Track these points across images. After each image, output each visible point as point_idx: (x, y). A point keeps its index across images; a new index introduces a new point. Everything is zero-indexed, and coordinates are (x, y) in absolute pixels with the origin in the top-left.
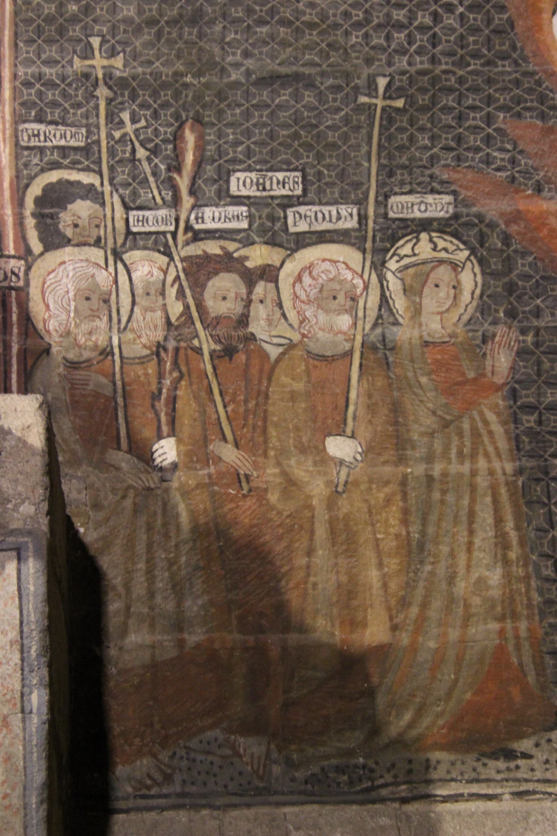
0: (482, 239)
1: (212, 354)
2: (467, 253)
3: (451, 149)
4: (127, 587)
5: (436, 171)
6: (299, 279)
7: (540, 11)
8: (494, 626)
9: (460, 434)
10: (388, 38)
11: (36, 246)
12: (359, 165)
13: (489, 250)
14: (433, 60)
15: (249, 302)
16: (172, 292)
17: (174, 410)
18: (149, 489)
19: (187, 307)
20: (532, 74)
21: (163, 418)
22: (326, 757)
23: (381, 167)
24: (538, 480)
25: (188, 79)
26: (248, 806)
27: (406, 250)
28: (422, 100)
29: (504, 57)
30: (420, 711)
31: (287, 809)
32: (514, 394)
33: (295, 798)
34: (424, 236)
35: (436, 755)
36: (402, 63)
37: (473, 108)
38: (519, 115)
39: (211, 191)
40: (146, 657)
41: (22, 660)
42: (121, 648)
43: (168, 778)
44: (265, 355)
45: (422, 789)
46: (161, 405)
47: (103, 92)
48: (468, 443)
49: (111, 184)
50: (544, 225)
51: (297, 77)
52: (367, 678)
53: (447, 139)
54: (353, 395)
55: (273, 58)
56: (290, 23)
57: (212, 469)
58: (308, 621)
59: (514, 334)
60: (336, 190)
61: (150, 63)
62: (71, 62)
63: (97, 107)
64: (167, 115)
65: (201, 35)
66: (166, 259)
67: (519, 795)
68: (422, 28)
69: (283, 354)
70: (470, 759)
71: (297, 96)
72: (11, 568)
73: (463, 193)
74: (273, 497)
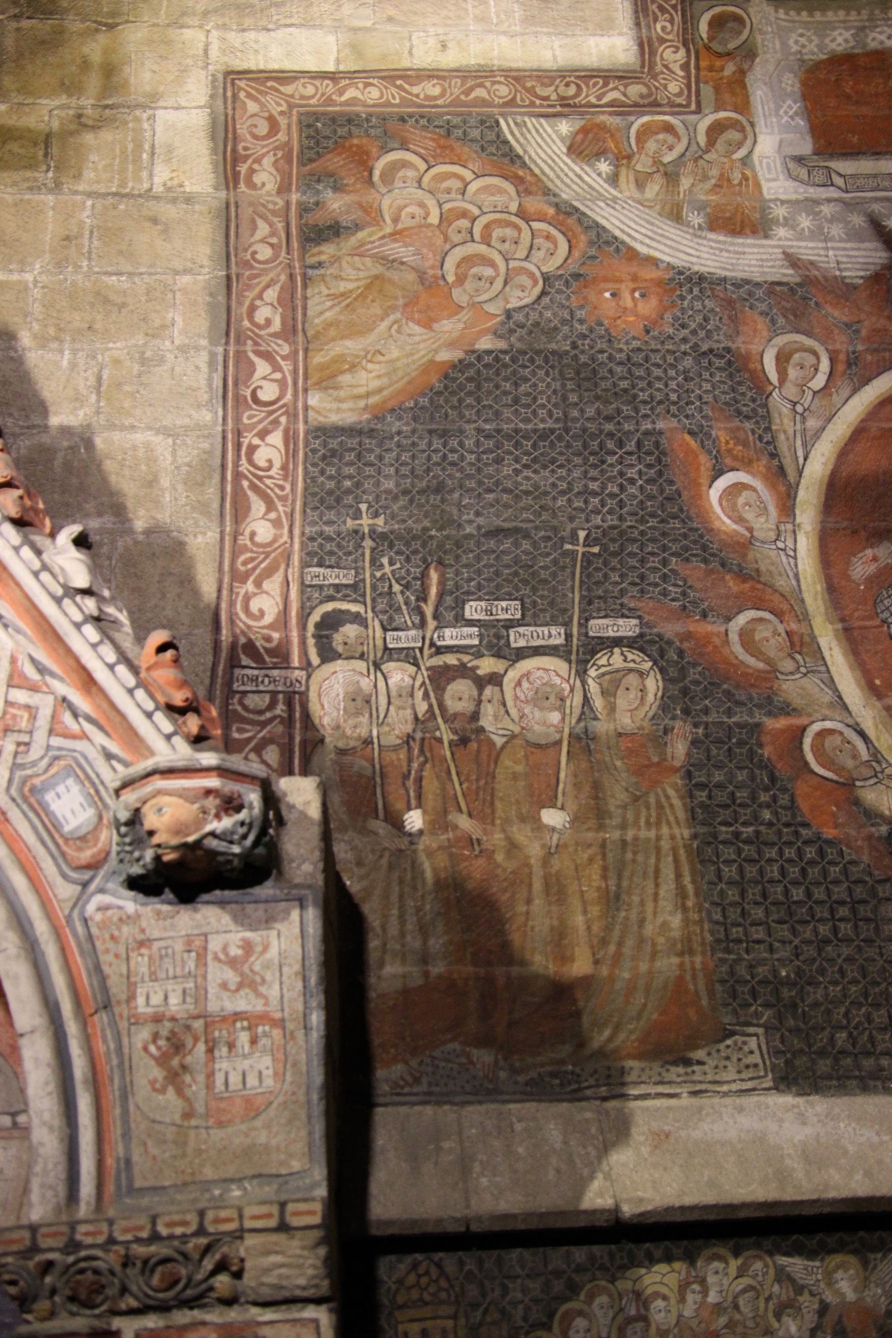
0: (662, 653)
1: (451, 743)
2: (650, 664)
3: (636, 584)
4: (384, 928)
5: (625, 600)
6: (519, 684)
7: (700, 485)
8: (675, 960)
9: (648, 808)
10: (586, 502)
11: (315, 660)
12: (565, 595)
13: (667, 661)
14: (621, 518)
15: (479, 702)
16: (419, 694)
17: (420, 787)
18: (401, 851)
19: (431, 706)
20: (697, 530)
21: (412, 794)
22: (542, 1065)
23: (582, 597)
24: (709, 843)
25: (433, 533)
26: (480, 1103)
27: (603, 661)
30: (617, 1028)
31: (512, 1106)
32: (689, 775)
33: (517, 1097)
34: (617, 650)
35: (630, 1063)
36: (597, 520)
37: (652, 554)
38: (687, 560)
39: (449, 616)
40: (398, 984)
41: (305, 987)
42: (379, 978)
43: (417, 1080)
44: (492, 744)
45: (618, 1090)
46: (410, 783)
48: (654, 814)
49: (373, 611)
50: (709, 642)
51: (517, 530)
52: (575, 1001)
53: (633, 577)
54: (562, 775)
55: (498, 516)
56: (510, 491)
57: (451, 835)
58: (528, 957)
59: (688, 727)
60: (548, 615)
61: (404, 521)
62: (345, 522)
63: (363, 555)
64: (417, 559)
65: (443, 501)
66: (414, 669)
67: (695, 1093)
68: (612, 496)
69: (506, 743)
70: (656, 1066)
71: (516, 544)
72: (295, 914)
73: (647, 618)
74: (499, 857)
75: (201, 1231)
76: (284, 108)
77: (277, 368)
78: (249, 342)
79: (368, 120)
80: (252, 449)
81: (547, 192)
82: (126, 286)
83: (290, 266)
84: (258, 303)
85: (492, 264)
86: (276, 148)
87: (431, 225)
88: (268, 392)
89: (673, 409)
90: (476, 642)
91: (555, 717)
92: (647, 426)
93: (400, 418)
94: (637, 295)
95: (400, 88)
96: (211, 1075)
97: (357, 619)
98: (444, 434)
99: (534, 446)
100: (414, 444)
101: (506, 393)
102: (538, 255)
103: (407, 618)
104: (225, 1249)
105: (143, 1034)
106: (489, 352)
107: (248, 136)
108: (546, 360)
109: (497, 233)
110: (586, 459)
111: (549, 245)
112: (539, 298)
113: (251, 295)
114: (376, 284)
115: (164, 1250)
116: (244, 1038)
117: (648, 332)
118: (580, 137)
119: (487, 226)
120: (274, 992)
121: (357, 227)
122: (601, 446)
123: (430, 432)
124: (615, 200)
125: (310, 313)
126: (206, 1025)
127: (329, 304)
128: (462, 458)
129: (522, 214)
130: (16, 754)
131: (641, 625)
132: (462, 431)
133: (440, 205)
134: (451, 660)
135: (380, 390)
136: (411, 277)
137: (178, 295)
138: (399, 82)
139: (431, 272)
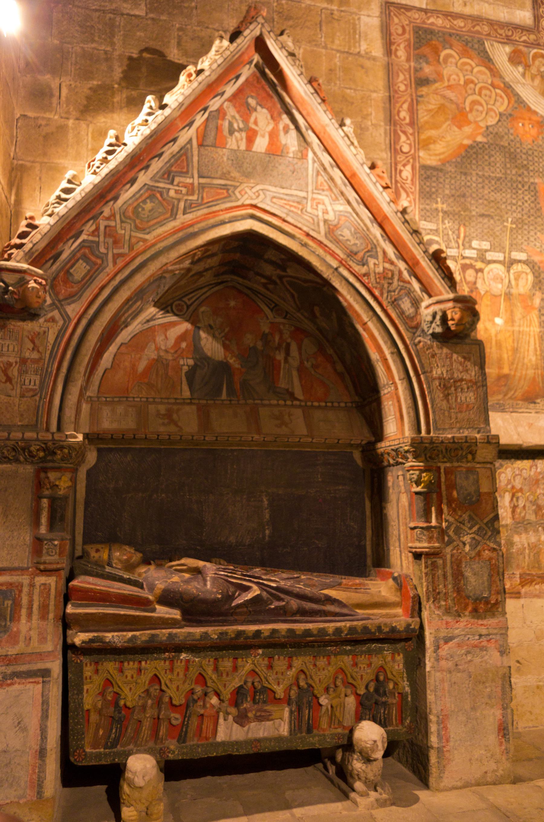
0: (533, 267)
6: (489, 273)
8: (533, 371)
13: (536, 270)
14: (522, 215)
15: (476, 278)
25: (462, 213)
28: (520, 226)
29: (539, 217)
30: (515, 391)
32: (540, 311)
36: (515, 215)
37: (532, 230)
44: (480, 293)
47: (441, 214)
53: (526, 238)
64: (457, 222)
67: (537, 413)
68: (520, 206)
70: (526, 403)
71: (489, 221)
75: (466, 442)
76: (407, 22)
77: (408, 139)
78: (398, 126)
79: (438, 33)
80: (401, 171)
81: (501, 77)
82: (353, 95)
83: (411, 95)
84: (401, 109)
85: (481, 105)
86: (405, 41)
87: (460, 85)
88: (406, 149)
89: (541, 175)
90: (475, 256)
91: (500, 286)
92: (532, 180)
93: (451, 165)
94: (530, 126)
95: (449, 20)
96: (456, 397)
97: (437, 243)
98: (465, 174)
99: (495, 183)
100: (456, 177)
101: (486, 160)
102: (498, 104)
103: (453, 244)
104: (473, 448)
105: (437, 383)
106: (480, 143)
107: (395, 34)
108: (500, 149)
109: (484, 92)
110: (512, 191)
111: (501, 100)
112: (497, 123)
113: (398, 105)
114: (442, 108)
115: (456, 446)
116: (465, 387)
117: (533, 142)
118: (512, 54)
119: (481, 89)
120: (473, 374)
121: (435, 81)
122: (517, 186)
123: (461, 173)
124: (524, 84)
125: (420, 116)
126: (455, 382)
127: (425, 114)
128: (471, 185)
129: (492, 85)
130: (388, 287)
131: (528, 256)
132: (471, 174)
133: (464, 76)
134: (468, 261)
135: (443, 153)
136: (454, 106)
137: (373, 102)
138: (449, 18)
139: (461, 105)
